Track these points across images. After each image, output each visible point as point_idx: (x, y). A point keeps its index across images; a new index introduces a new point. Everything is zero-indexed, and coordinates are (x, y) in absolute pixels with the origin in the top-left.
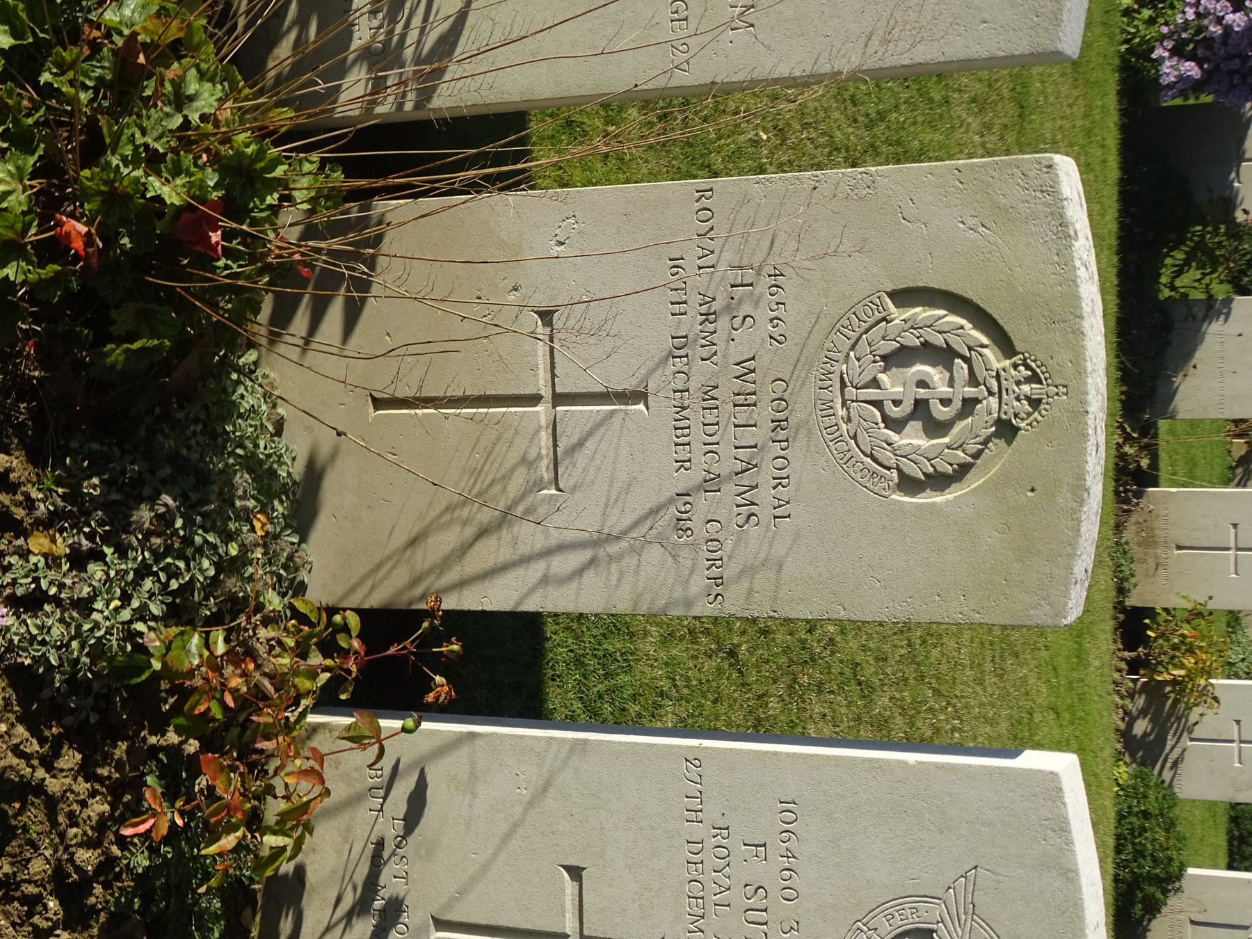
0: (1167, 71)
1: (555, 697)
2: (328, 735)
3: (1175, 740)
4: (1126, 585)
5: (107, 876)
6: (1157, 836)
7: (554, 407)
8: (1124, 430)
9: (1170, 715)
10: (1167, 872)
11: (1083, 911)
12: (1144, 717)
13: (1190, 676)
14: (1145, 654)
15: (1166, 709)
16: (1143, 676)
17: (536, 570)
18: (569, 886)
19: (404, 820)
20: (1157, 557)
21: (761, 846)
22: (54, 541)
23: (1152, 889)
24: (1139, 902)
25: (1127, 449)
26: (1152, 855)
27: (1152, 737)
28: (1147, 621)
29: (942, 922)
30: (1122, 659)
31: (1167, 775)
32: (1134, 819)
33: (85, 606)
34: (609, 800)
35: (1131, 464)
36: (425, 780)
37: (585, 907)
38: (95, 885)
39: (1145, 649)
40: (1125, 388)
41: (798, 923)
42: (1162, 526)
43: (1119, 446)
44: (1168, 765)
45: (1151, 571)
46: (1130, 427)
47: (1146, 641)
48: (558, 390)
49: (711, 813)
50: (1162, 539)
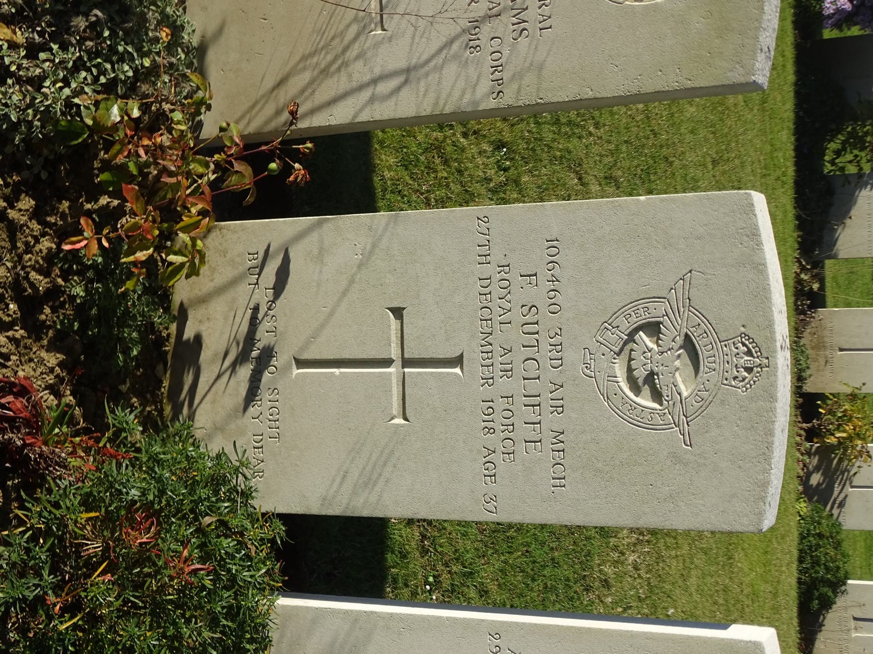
0: (828, 6)
1: (380, 204)
2: (219, 232)
3: (840, 487)
4: (803, 374)
5: (54, 302)
6: (828, 551)
8: (800, 263)
9: (836, 470)
10: (836, 577)
11: (770, 293)
12: (818, 472)
13: (850, 438)
14: (818, 425)
15: (834, 466)
16: (816, 443)
17: (366, 95)
18: (394, 323)
19: (273, 289)
20: (826, 357)
21: (533, 275)
22: (15, 33)
23: (825, 589)
24: (816, 599)
25: (803, 276)
26: (824, 564)
27: (824, 486)
28: (819, 402)
29: (667, 315)
30: (801, 428)
31: (835, 512)
32: (811, 539)
33: (37, 83)
34: (422, 256)
35: (806, 287)
36: (289, 257)
37: (405, 337)
38: (45, 307)
40: (801, 233)
41: (560, 329)
42: (829, 335)
43: (798, 275)
44: (836, 505)
46: (805, 261)
47: (819, 416)
48: (406, 356)
49: (497, 257)
50: (829, 344)
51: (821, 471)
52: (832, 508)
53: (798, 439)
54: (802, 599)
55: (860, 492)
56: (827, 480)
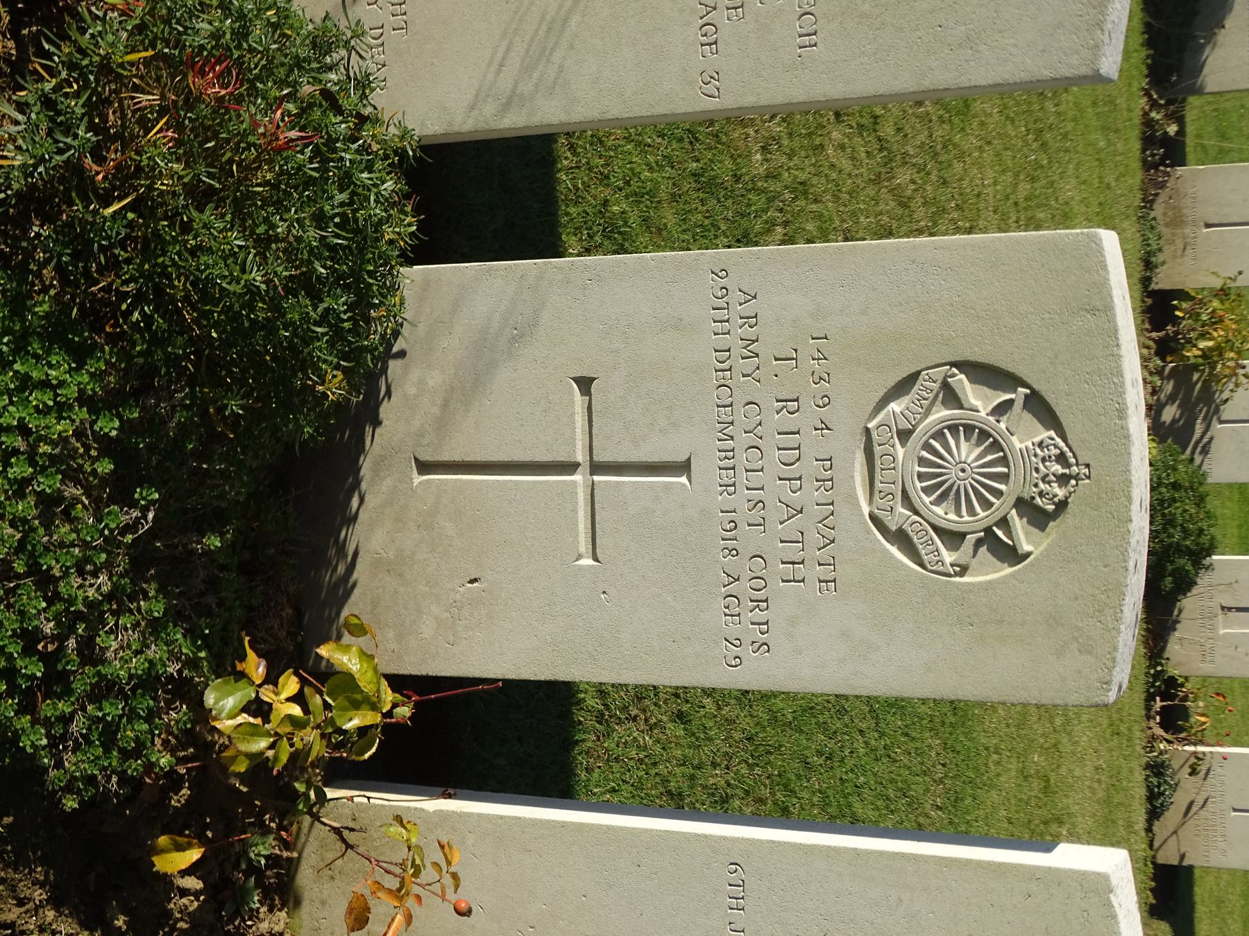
4: (1153, 259)
8: (1150, 96)
12: (1173, 403)
13: (1219, 350)
14: (1173, 332)
16: (1171, 362)
20: (1185, 238)
25: (1153, 114)
27: (1181, 422)
28: (1175, 302)
30: (1150, 338)
31: (1198, 459)
39: (1173, 326)
40: (1152, 52)
42: (1190, 205)
43: (1146, 114)
44: (1199, 449)
45: (1179, 253)
46: (1157, 92)
47: (1176, 321)
51: (1178, 402)
52: (1193, 453)
53: (1145, 351)
55: (1233, 429)
56: (1186, 413)
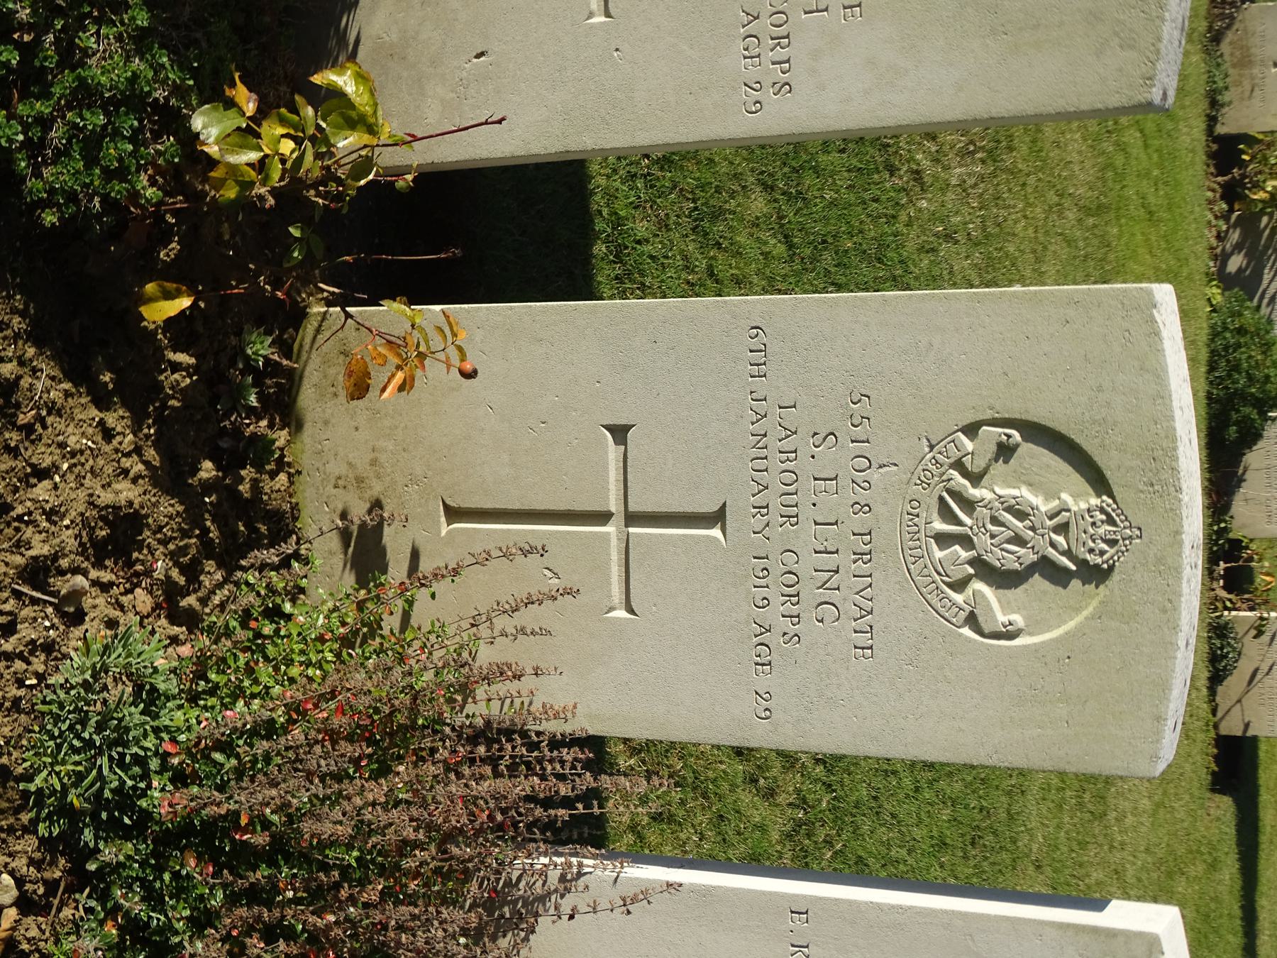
3: (1272, 273)
4: (1219, 98)
7: (627, 526)
9: (1267, 247)
12: (1239, 253)
15: (1263, 242)
20: (1253, 78)
27: (1248, 272)
28: (1241, 146)
30: (1215, 182)
39: (1240, 169)
44: (1265, 301)
45: (1247, 94)
50: (1259, 58)
53: (1210, 194)
54: (1213, 424)
56: (1252, 264)
